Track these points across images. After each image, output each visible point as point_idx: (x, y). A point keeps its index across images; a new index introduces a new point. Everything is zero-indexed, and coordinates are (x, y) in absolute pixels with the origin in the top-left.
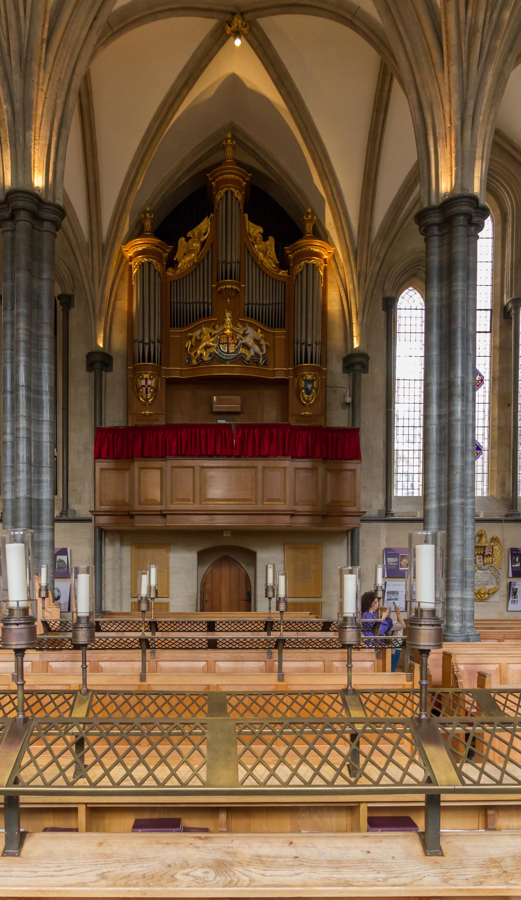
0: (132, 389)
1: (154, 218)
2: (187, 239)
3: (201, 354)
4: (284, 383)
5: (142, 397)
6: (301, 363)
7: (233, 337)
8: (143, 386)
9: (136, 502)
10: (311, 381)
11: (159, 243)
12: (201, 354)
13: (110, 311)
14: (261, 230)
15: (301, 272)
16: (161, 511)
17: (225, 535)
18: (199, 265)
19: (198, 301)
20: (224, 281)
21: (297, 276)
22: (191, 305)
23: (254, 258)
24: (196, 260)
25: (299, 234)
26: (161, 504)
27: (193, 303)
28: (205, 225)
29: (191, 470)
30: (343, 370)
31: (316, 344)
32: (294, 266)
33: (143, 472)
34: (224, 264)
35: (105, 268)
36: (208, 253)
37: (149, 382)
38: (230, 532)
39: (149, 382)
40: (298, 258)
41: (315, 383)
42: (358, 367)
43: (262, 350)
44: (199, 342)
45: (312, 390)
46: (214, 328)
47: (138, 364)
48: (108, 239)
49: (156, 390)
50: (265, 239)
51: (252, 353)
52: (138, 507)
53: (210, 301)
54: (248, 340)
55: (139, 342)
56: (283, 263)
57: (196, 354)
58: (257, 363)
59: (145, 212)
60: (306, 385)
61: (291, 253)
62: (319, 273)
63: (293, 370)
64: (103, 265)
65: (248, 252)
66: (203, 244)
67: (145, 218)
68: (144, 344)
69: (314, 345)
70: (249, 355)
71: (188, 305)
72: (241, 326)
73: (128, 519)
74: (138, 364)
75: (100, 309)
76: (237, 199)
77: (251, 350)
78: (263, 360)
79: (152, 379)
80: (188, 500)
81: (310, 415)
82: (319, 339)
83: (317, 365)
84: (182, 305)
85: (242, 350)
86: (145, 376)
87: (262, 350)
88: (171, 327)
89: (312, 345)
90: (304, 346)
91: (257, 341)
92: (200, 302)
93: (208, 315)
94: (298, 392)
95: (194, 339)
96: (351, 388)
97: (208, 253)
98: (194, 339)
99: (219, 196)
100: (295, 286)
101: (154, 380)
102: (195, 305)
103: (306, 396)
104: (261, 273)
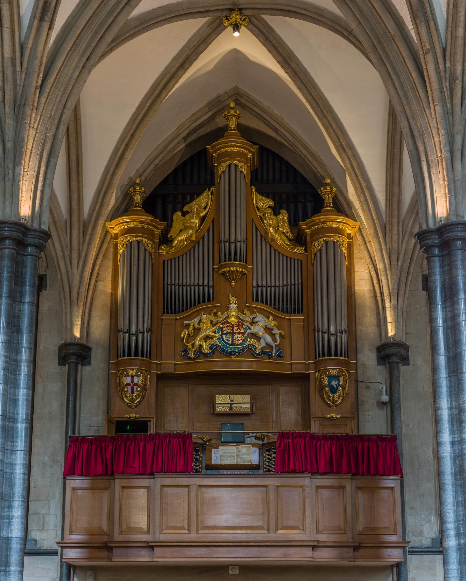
0: (113, 389)
1: (144, 191)
2: (184, 214)
3: (201, 346)
4: (305, 378)
5: (127, 397)
6: (324, 356)
7: (238, 326)
8: (128, 384)
9: (116, 531)
10: (337, 378)
11: (151, 220)
12: (201, 346)
13: (90, 293)
14: (271, 203)
15: (320, 250)
16: (147, 542)
17: (231, 572)
18: (198, 243)
19: (196, 283)
20: (227, 262)
21: (315, 254)
22: (189, 288)
23: (264, 237)
24: (194, 239)
25: (318, 206)
26: (148, 533)
27: (190, 285)
28: (205, 199)
29: (187, 489)
30: (377, 361)
31: (341, 333)
32: (312, 242)
33: (126, 492)
34: (227, 244)
35: (85, 246)
36: (208, 230)
37: (136, 380)
38: (237, 567)
39: (136, 380)
40: (316, 234)
41: (341, 379)
42: (394, 359)
43: (275, 341)
44: (197, 331)
45: (337, 387)
46: (215, 314)
47: (122, 358)
48: (90, 215)
49: (144, 389)
50: (276, 212)
51: (263, 344)
52: (118, 537)
53: (211, 284)
54: (258, 329)
55: (124, 332)
56: (299, 239)
57: (193, 345)
58: (270, 356)
59: (135, 184)
60: (330, 382)
61: (308, 228)
62: (341, 250)
63: (314, 363)
64: (83, 244)
65: (256, 228)
66: (203, 219)
67: (135, 192)
68: (130, 335)
69: (339, 334)
71: (185, 287)
72: (248, 313)
73: (105, 553)
74: (122, 358)
75: (78, 292)
76: (241, 172)
77: (262, 341)
78: (276, 352)
79: (139, 376)
80: (182, 528)
81: (337, 418)
82: (344, 326)
83: (343, 358)
84: (177, 287)
85: (250, 341)
86: (131, 372)
87: (275, 341)
88: (164, 313)
89: (335, 334)
90: (326, 336)
91: (268, 330)
92: (198, 285)
93: (209, 300)
94: (321, 389)
95: (191, 328)
96: (388, 384)
97: (208, 230)
98: (191, 328)
100: (313, 264)
101: (141, 377)
102: (193, 287)
103: (330, 394)
104: (273, 250)
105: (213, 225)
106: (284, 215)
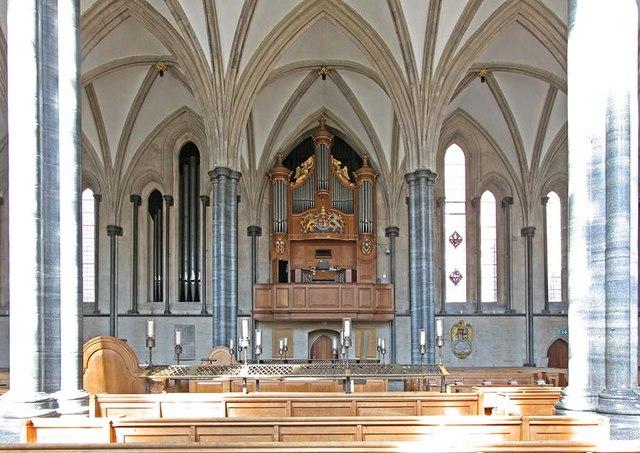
0: (273, 245)
25: (360, 163)
28: (310, 160)
44: (308, 221)
50: (342, 167)
54: (334, 221)
56: (352, 180)
70: (335, 228)
91: (339, 221)
99: (318, 146)
105: (314, 172)
106: (346, 168)
